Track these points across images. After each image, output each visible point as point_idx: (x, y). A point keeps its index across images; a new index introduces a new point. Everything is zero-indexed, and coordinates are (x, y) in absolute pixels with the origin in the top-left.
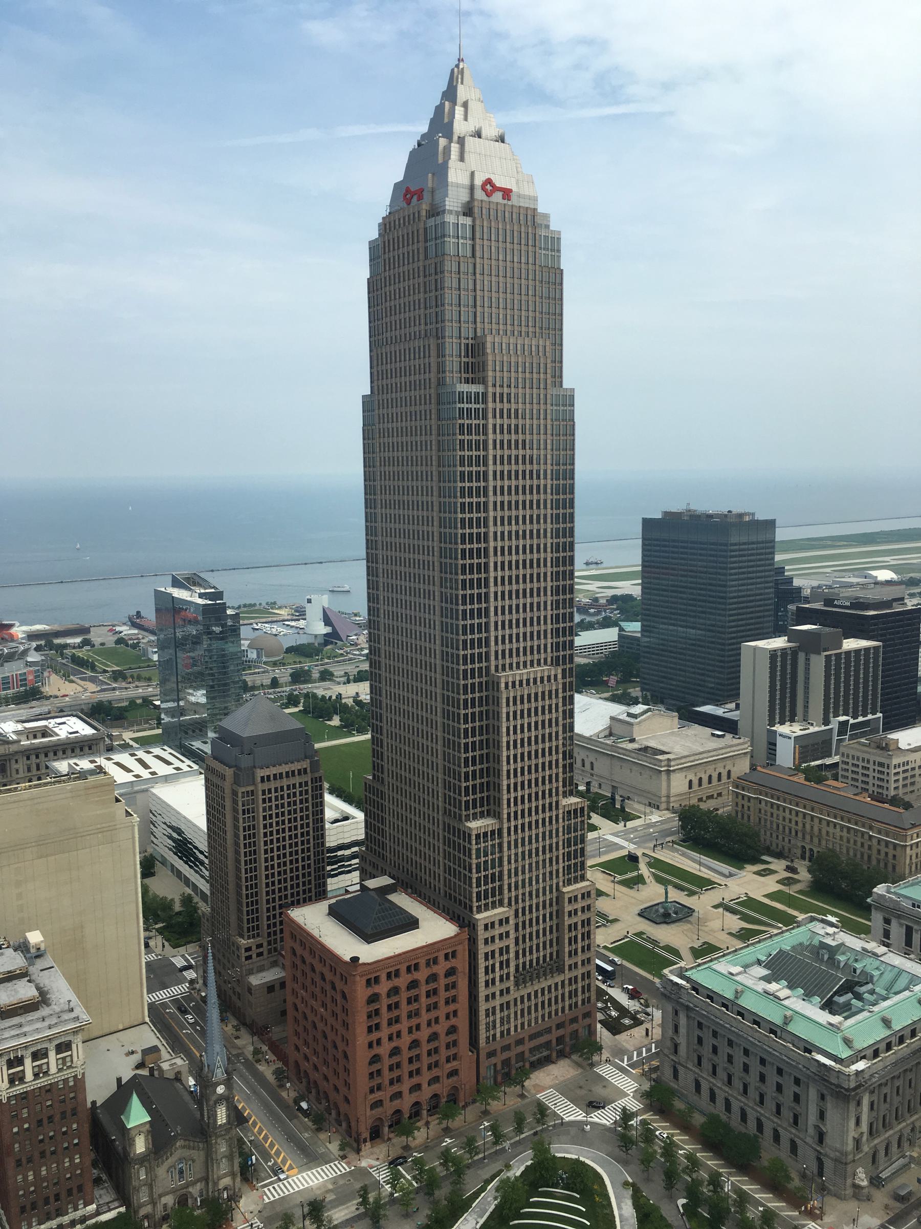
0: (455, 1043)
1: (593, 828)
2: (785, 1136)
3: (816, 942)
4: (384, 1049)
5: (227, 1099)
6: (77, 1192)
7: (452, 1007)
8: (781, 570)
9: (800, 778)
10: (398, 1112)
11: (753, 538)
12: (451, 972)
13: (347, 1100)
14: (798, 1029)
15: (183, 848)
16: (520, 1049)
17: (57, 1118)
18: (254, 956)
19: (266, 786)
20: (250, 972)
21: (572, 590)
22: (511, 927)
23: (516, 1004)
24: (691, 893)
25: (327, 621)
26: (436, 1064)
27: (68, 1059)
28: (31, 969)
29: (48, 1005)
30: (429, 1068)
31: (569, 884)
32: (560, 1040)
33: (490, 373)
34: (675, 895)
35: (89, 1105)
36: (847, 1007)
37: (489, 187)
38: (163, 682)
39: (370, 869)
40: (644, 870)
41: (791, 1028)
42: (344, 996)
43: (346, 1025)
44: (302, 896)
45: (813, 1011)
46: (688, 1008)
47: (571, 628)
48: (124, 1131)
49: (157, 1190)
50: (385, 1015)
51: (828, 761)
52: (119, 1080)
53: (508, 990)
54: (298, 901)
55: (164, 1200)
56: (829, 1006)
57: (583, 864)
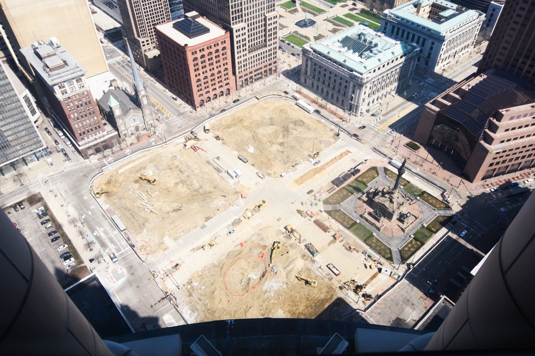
0: (227, 74)
2: (340, 99)
4: (202, 77)
12: (224, 48)
14: (349, 64)
16: (251, 75)
22: (246, 31)
26: (221, 81)
30: (219, 82)
32: (266, 71)
34: (310, 16)
44: (161, 21)
46: (311, 58)
48: (111, 108)
49: (127, 126)
50: (200, 65)
52: (104, 91)
53: (246, 55)
54: (160, 22)
55: (130, 129)
56: (361, 56)
57: (274, 4)
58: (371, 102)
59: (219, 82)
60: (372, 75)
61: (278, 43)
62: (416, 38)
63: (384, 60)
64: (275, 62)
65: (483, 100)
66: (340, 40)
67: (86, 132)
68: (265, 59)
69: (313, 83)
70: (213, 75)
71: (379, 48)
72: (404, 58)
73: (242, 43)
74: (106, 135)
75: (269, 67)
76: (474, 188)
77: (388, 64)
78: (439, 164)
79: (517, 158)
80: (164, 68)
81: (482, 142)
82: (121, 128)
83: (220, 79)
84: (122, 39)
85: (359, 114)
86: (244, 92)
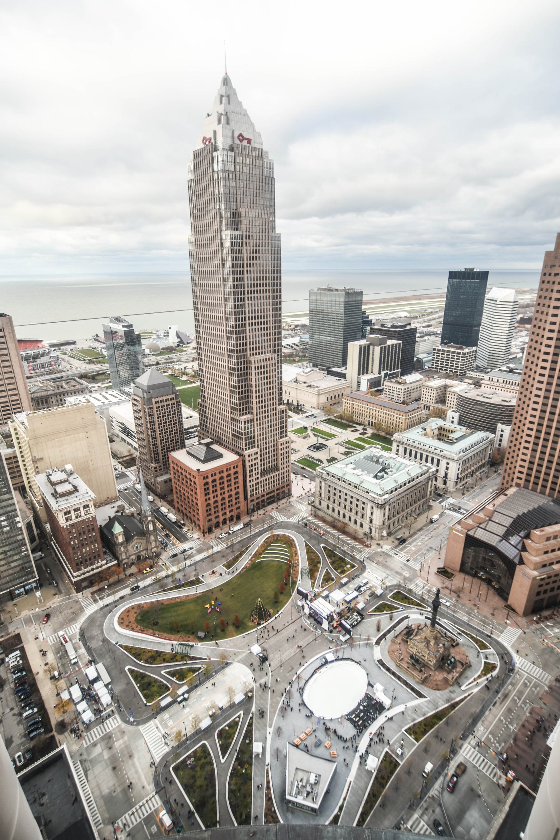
0: (238, 498)
1: (290, 417)
3: (372, 455)
4: (212, 501)
7: (237, 485)
8: (364, 313)
9: (369, 396)
10: (218, 522)
11: (354, 299)
12: (236, 473)
13: (198, 519)
15: (126, 431)
16: (263, 498)
17: (87, 532)
19: (157, 405)
20: (157, 476)
21: (281, 322)
22: (259, 456)
24: (327, 440)
25: (178, 337)
26: (232, 505)
28: (70, 479)
30: (229, 506)
31: (281, 438)
32: (278, 494)
33: (243, 226)
36: (383, 477)
37: (241, 138)
38: (110, 363)
39: (202, 436)
40: (309, 431)
42: (195, 483)
43: (196, 493)
47: (281, 338)
50: (211, 489)
51: (379, 388)
52: (109, 517)
55: (132, 557)
56: (376, 477)
58: (392, 525)
62: (430, 459)
63: (401, 481)
67: (84, 561)
74: (104, 565)
75: (281, 490)
80: (174, 492)
86: (255, 517)
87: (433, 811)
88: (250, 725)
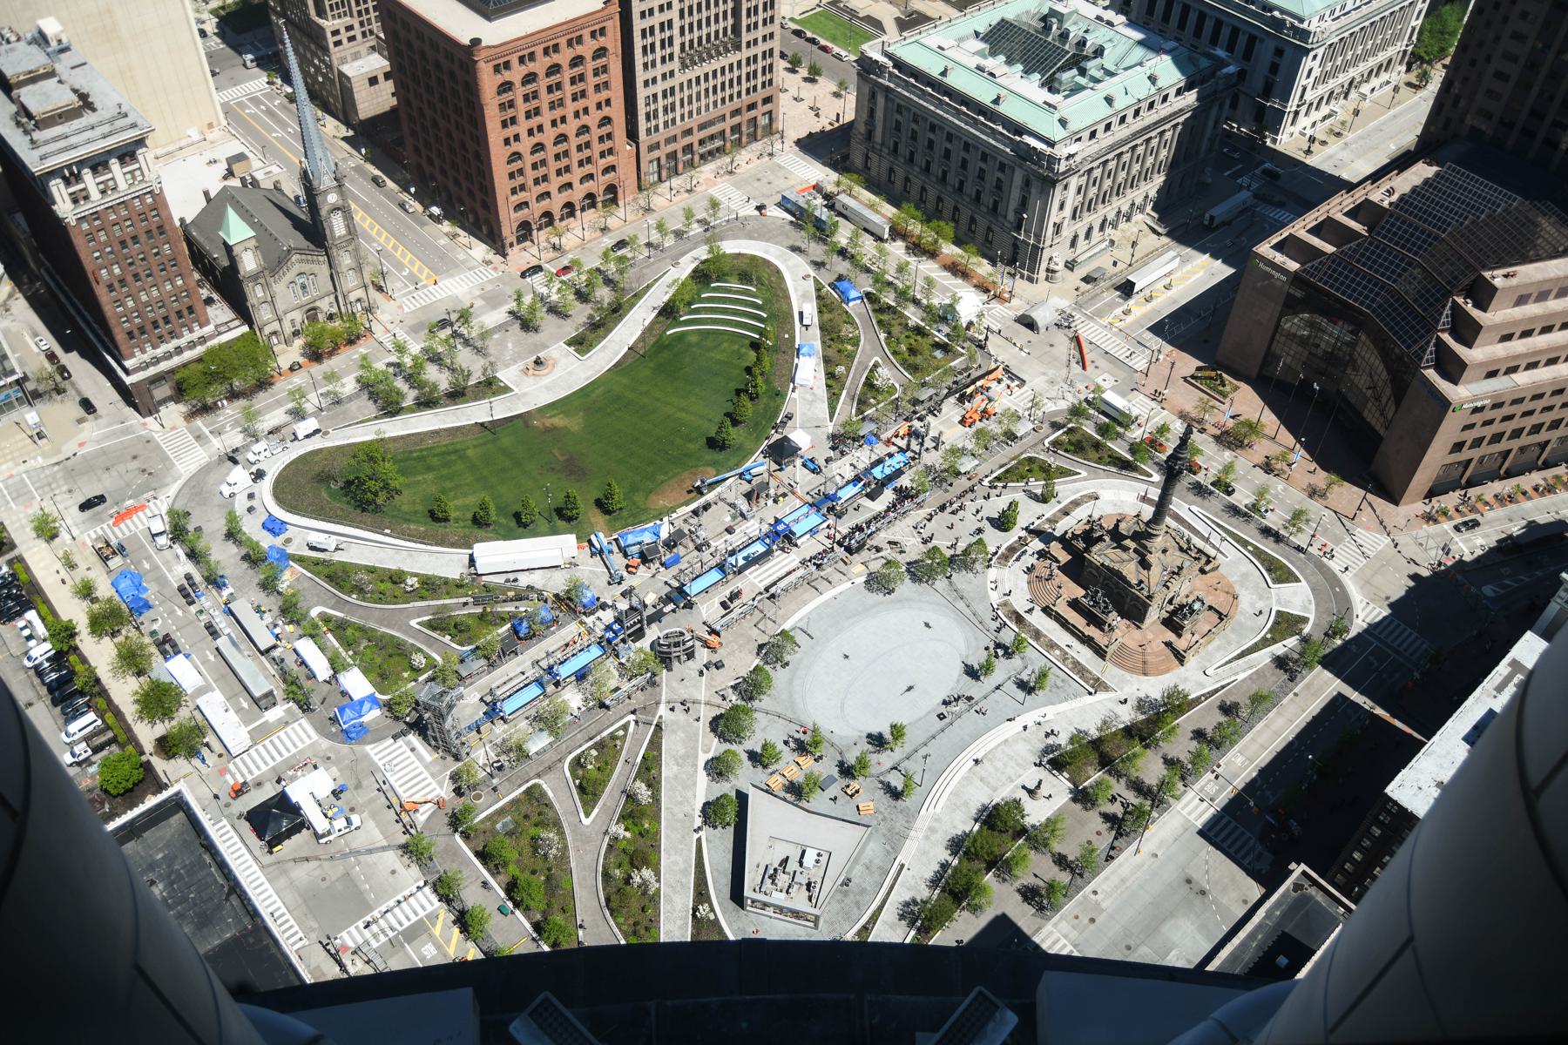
0: (609, 136)
2: (983, 223)
3: (1045, 11)
5: (343, 209)
6: (190, 313)
7: (604, 95)
12: (601, 52)
18: (345, 41)
20: (343, 61)
23: (682, 89)
26: (589, 160)
27: (138, 173)
28: (58, 67)
29: (94, 110)
30: (581, 164)
32: (736, 129)
35: (178, 224)
41: (1003, 109)
45: (1032, 87)
49: (281, 307)
50: (522, 107)
52: (206, 194)
53: (672, 73)
55: (290, 316)
56: (1051, 85)
59: (581, 164)
60: (1084, 149)
61: (777, 37)
62: (1225, 32)
64: (767, 100)
65: (1435, 239)
66: (982, 30)
67: (149, 327)
68: (736, 89)
69: (891, 170)
70: (562, 138)
71: (1108, 61)
72: (1191, 98)
73: (658, 36)
74: (212, 337)
76: (1404, 522)
77: (1137, 113)
78: (1299, 441)
79: (1536, 429)
81: (1431, 374)
82: (263, 314)
83: (587, 153)
84: (270, 22)
85: (1042, 274)
87: (1092, 920)
88: (655, 744)
